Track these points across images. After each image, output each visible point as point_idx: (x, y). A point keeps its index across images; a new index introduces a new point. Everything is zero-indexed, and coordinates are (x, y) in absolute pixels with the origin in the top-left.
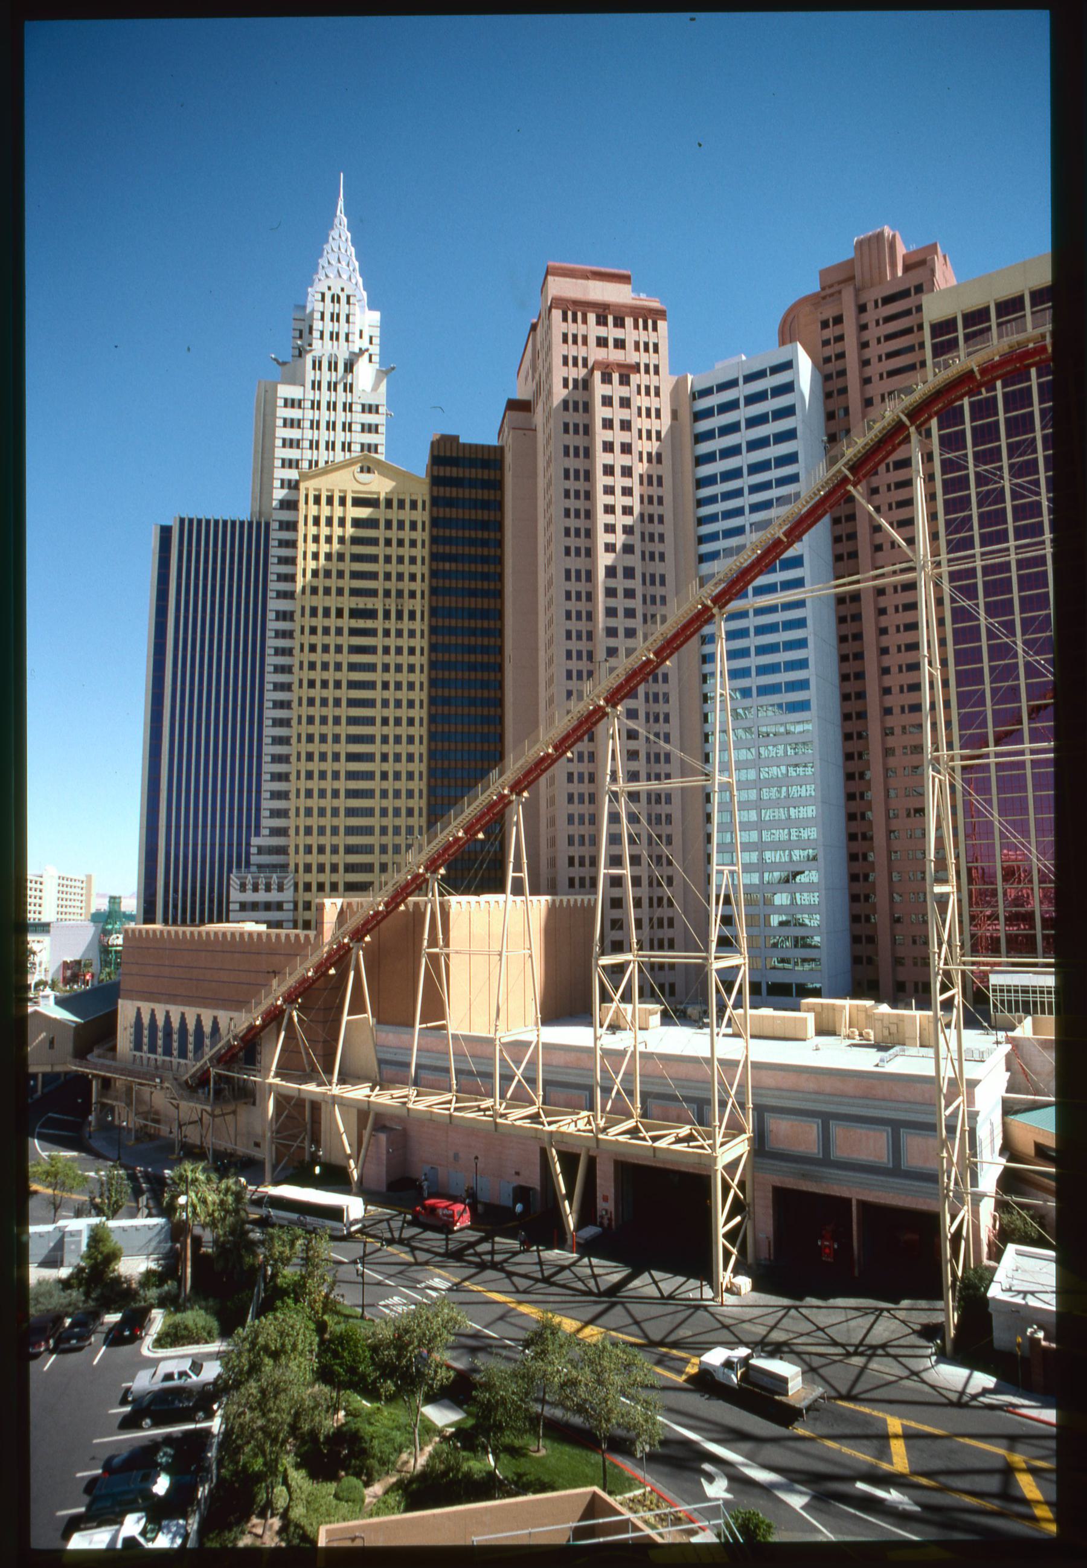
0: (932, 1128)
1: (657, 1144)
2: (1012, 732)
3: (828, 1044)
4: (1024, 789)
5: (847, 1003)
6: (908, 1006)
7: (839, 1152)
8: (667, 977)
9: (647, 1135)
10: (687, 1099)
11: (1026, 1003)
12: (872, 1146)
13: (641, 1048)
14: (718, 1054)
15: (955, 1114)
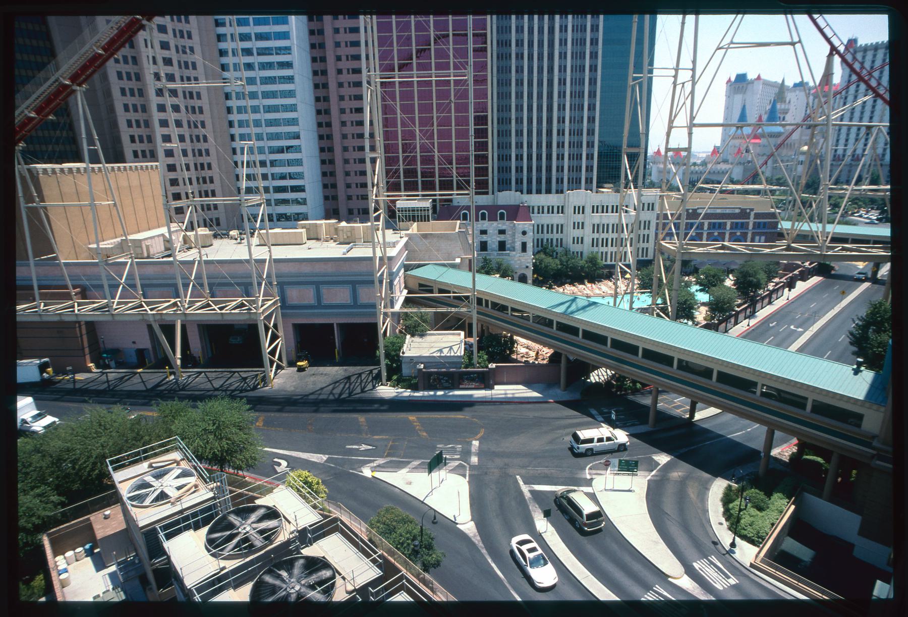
0: (372, 282)
1: (223, 311)
2: (407, 64)
3: (317, 245)
4: (413, 99)
5: (323, 222)
6: (355, 222)
7: (325, 302)
8: (213, 214)
9: (216, 308)
10: (239, 284)
11: (414, 216)
12: (342, 296)
13: (204, 258)
14: (254, 257)
15: (382, 275)
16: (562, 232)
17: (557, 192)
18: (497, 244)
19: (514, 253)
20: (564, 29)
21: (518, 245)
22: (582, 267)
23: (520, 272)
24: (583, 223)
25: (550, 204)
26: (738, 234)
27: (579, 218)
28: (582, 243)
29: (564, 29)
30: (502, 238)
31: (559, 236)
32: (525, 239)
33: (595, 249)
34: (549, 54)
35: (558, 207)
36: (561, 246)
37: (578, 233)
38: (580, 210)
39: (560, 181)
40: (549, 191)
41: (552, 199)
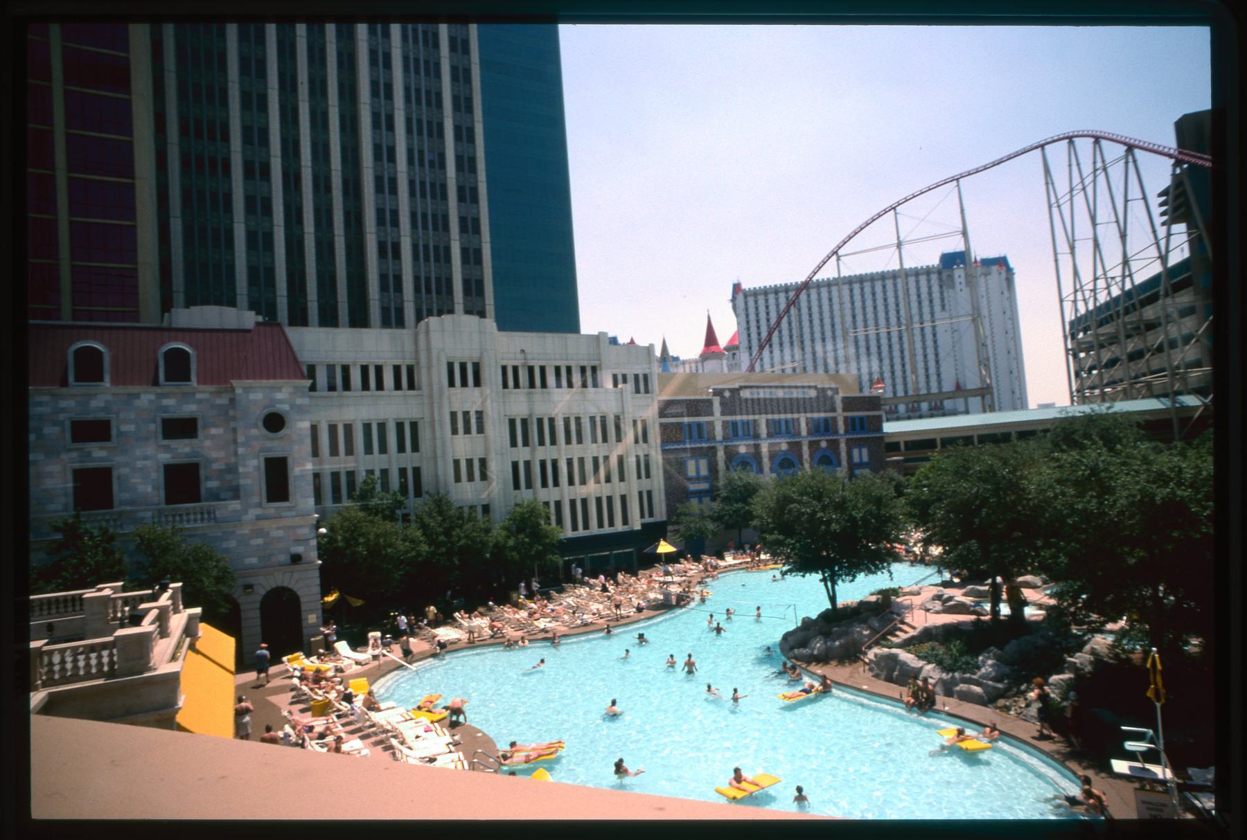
16: (415, 448)
17: (386, 323)
18: (158, 477)
19: (235, 505)
20: (381, 60)
21: (252, 472)
22: (499, 548)
23: (265, 584)
24: (480, 415)
25: (371, 360)
26: (824, 444)
27: (466, 399)
28: (484, 476)
29: (381, 60)
30: (182, 449)
31: (409, 460)
32: (276, 446)
33: (525, 495)
34: (345, 182)
35: (397, 369)
36: (418, 492)
37: (463, 447)
38: (467, 374)
39: (391, 283)
40: (359, 319)
41: (376, 345)
